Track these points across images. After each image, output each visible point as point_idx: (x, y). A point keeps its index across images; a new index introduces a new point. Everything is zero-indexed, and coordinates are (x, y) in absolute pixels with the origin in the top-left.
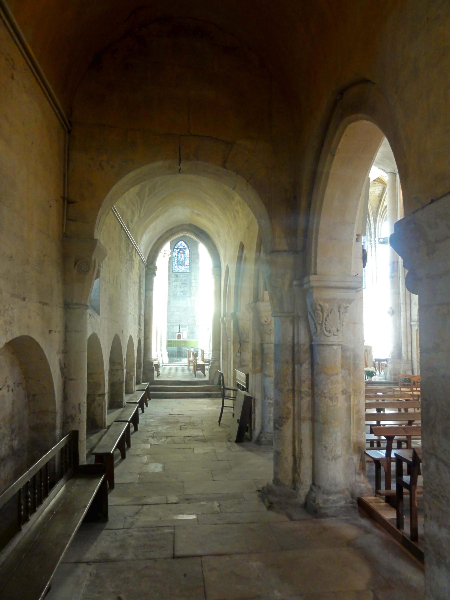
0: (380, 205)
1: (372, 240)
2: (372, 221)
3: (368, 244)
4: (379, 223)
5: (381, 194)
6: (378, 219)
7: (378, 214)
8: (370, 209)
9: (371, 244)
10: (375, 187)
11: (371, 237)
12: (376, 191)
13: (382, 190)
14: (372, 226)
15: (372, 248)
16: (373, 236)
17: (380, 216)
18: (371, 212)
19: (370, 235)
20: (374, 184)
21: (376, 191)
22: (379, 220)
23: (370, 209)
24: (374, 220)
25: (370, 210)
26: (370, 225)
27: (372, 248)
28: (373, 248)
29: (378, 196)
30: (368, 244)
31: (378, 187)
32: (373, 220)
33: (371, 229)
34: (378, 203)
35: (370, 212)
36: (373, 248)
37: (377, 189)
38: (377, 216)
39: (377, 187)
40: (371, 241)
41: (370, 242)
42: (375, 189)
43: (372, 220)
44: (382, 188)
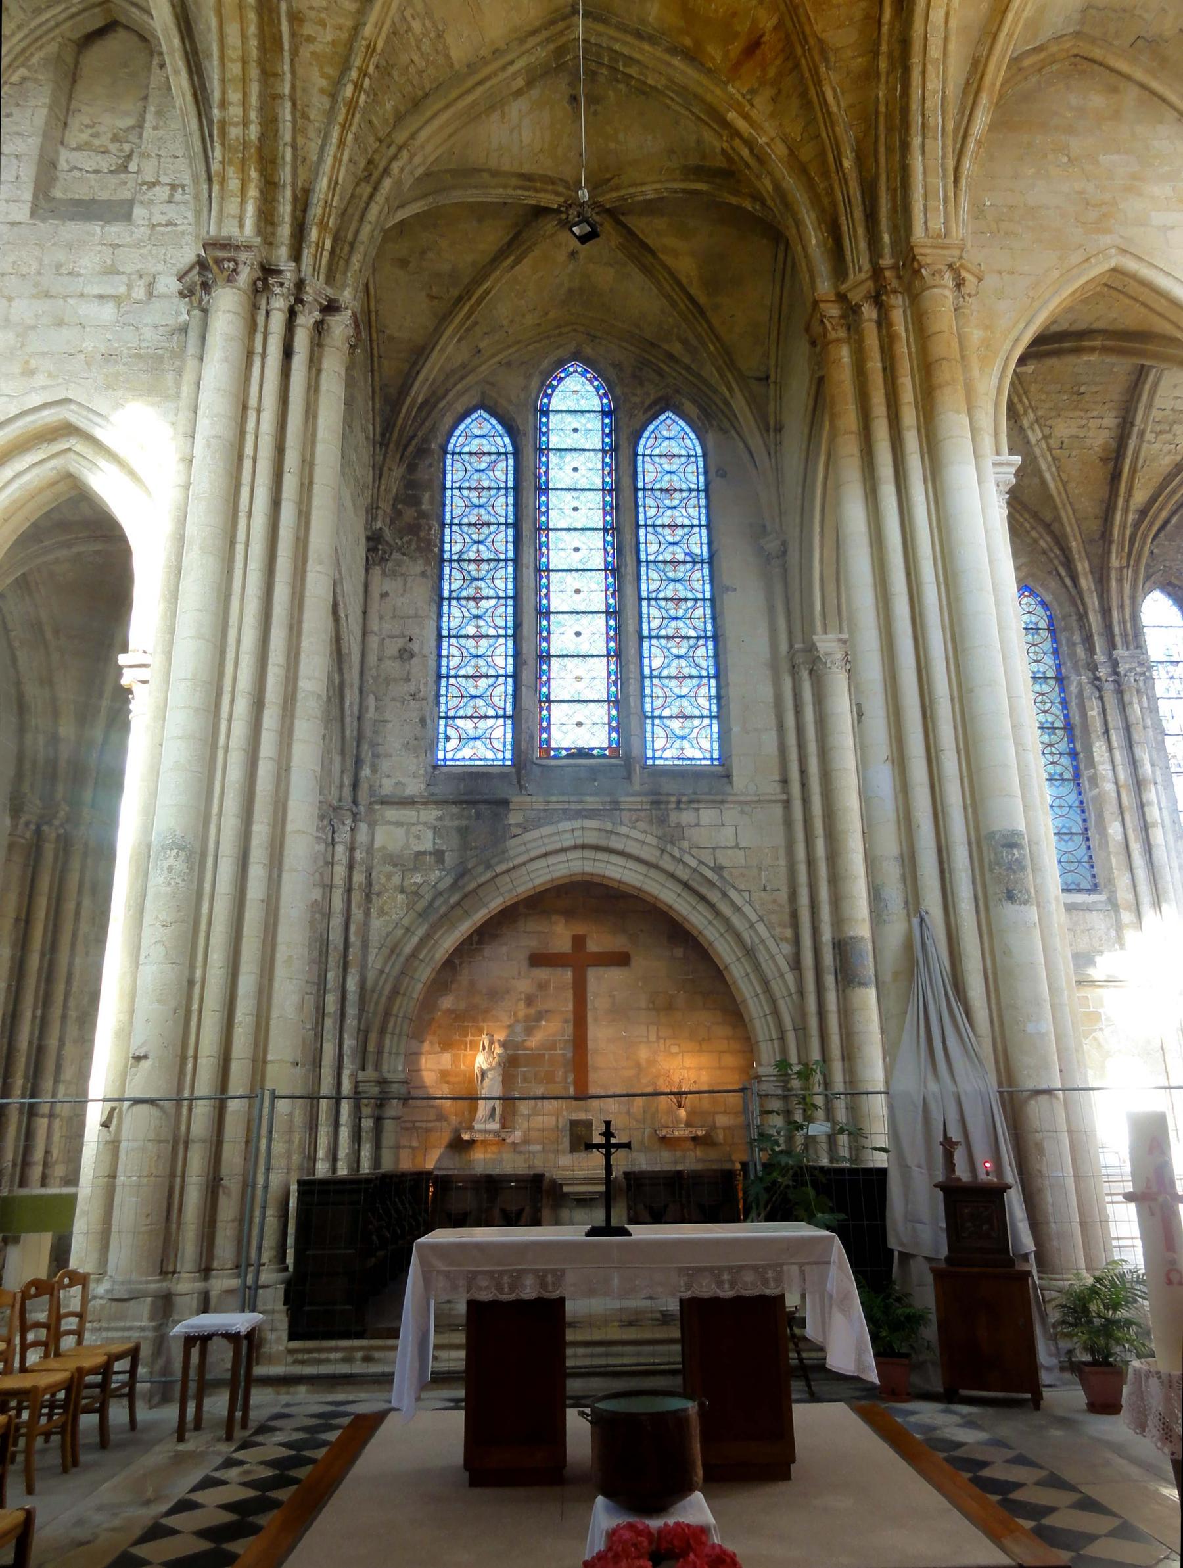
0: (1117, 495)
1: (1100, 657)
2: (1087, 578)
3: (1080, 683)
4: (1120, 581)
5: (1114, 445)
6: (1115, 562)
7: (1111, 542)
8: (1070, 524)
9: (1097, 679)
10: (1082, 414)
11: (1091, 650)
12: (1091, 434)
13: (1118, 426)
14: (1088, 600)
15: (1101, 698)
16: (1099, 643)
17: (1122, 550)
18: (1074, 536)
19: (1084, 645)
20: (1075, 397)
21: (1091, 434)
22: (1121, 569)
23: (1070, 524)
24: (1097, 575)
25: (1073, 530)
26: (1077, 597)
27: (1101, 698)
28: (1111, 700)
29: (1101, 459)
30: (1080, 683)
31: (1095, 413)
32: (1092, 573)
33: (1086, 613)
34: (1104, 492)
35: (1071, 539)
36: (1111, 700)
37: (1093, 424)
38: (1109, 552)
39: (1089, 415)
40: (1093, 667)
41: (1090, 674)
42: (1085, 422)
43: (1086, 574)
44: (1113, 414)
